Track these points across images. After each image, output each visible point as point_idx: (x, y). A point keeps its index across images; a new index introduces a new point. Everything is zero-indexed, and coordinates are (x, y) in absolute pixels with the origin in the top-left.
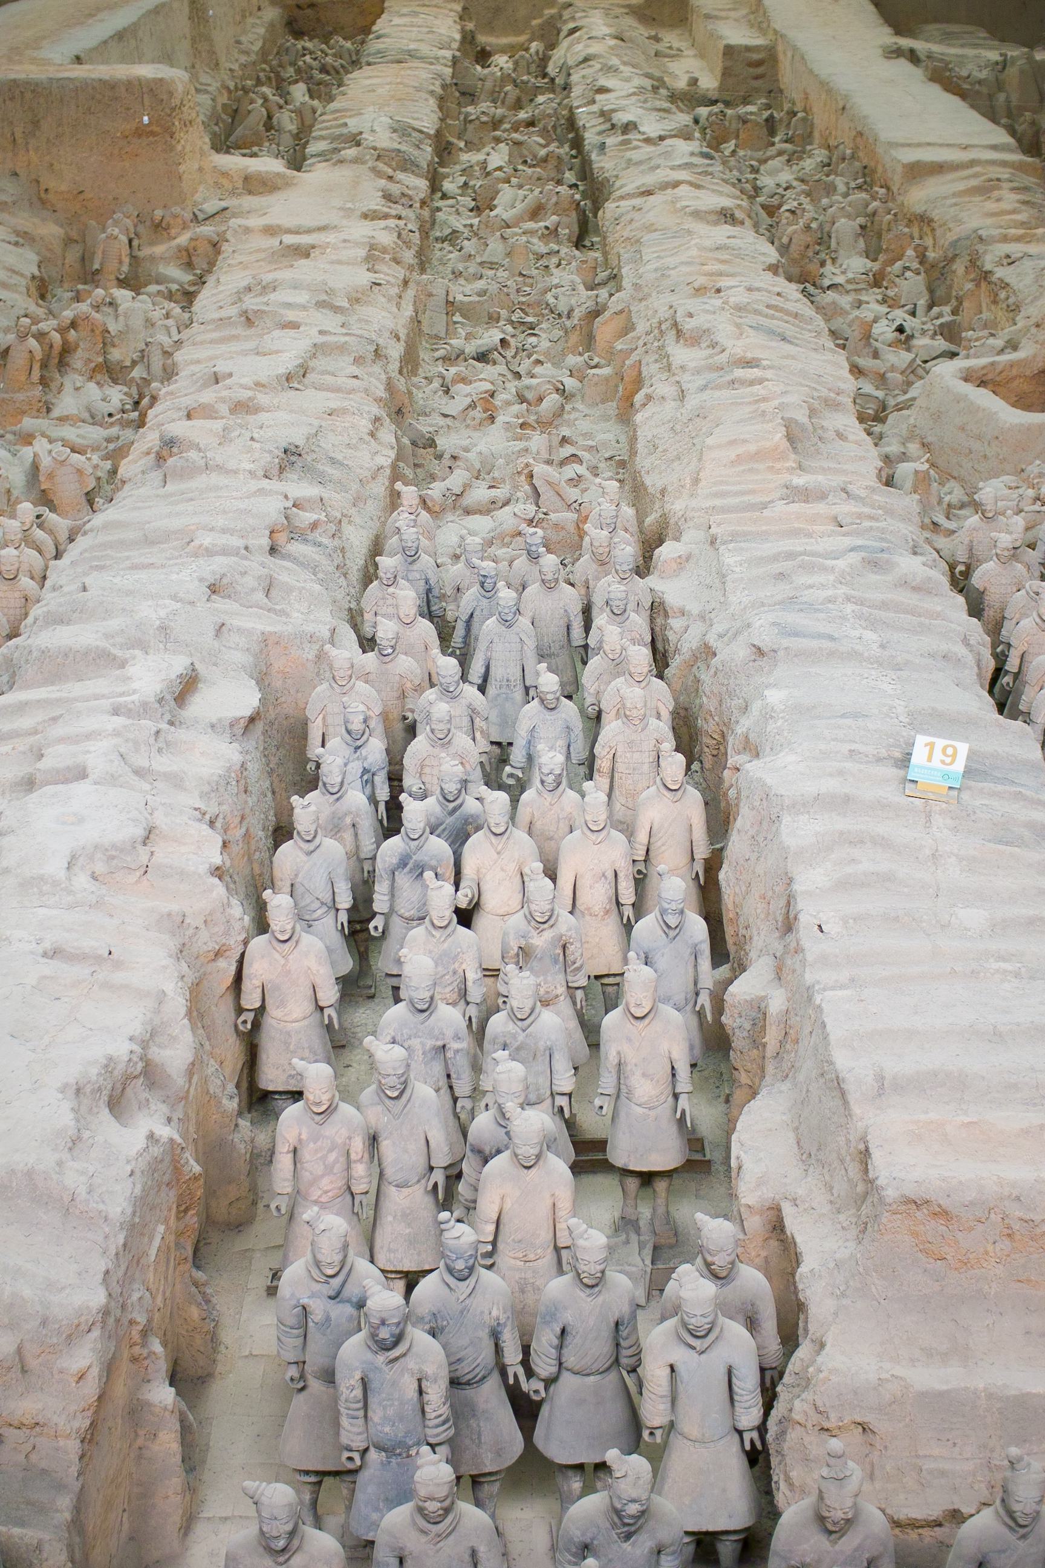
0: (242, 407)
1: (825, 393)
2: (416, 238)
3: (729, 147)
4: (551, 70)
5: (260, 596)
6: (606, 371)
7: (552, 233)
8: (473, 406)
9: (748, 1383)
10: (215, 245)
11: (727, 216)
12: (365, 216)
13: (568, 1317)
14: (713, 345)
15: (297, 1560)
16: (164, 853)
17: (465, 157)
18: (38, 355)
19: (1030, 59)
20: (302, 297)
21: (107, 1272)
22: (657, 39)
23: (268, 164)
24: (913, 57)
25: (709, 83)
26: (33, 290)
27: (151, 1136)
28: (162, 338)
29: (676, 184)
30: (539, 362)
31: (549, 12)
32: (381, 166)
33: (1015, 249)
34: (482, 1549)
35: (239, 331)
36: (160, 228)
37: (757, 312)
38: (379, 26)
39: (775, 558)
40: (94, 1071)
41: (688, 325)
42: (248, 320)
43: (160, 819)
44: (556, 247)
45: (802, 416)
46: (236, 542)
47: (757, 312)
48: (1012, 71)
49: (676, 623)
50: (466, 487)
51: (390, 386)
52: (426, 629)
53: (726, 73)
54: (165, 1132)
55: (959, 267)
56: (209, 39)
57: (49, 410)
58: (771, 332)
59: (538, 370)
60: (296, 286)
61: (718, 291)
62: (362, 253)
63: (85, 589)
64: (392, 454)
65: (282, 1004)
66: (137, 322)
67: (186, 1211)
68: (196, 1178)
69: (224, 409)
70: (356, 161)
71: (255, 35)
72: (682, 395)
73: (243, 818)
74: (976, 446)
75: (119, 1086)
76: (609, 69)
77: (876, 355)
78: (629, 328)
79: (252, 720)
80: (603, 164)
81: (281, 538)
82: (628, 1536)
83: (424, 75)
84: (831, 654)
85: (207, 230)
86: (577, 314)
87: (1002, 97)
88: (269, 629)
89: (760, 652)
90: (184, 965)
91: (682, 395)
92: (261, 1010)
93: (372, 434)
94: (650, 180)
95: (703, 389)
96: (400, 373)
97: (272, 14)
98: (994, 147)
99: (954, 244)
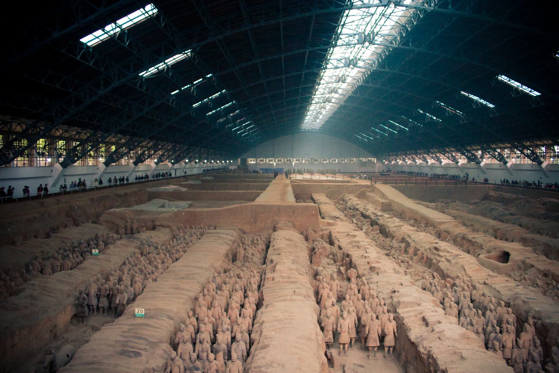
6: (416, 257)
12: (354, 230)
14: (448, 252)
20: (365, 243)
24: (420, 203)
29: (402, 225)
33: (476, 236)
35: (357, 249)
41: (442, 248)
53: (382, 207)
55: (459, 240)
60: (363, 242)
61: (437, 243)
63: (398, 292)
72: (448, 261)
78: (416, 250)
80: (381, 222)
85: (326, 232)
86: (402, 247)
91: (448, 261)
94: (397, 224)
95: (454, 259)
99: (456, 235)
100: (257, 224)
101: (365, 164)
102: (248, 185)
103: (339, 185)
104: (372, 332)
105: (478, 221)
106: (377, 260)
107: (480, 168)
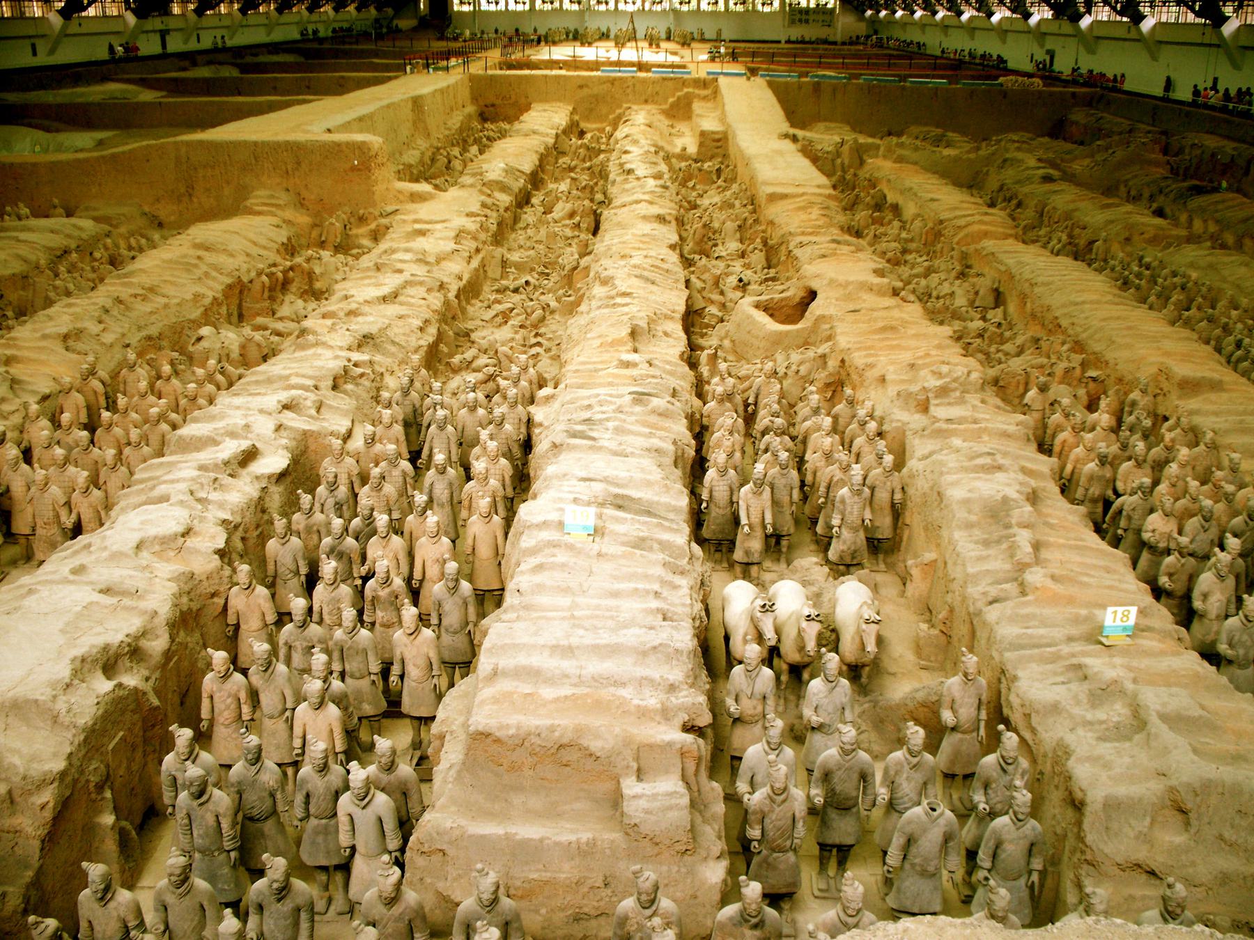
0: (352, 313)
1: (665, 311)
2: (494, 228)
3: (691, 184)
4: (612, 140)
5: (313, 412)
7: (578, 226)
8: (496, 315)
9: (390, 825)
10: (388, 228)
11: (661, 219)
12: (467, 215)
13: (309, 786)
15: (112, 905)
16: (191, 542)
17: (552, 186)
18: (267, 284)
19: (856, 140)
21: (71, 754)
22: (672, 126)
23: (424, 187)
24: (794, 139)
25: (692, 149)
26: (282, 250)
27: (120, 685)
28: (338, 277)
29: (637, 202)
30: (543, 293)
31: (618, 111)
32: (485, 189)
33: (805, 239)
34: (205, 904)
36: (362, 220)
37: (644, 269)
38: (525, 117)
39: (589, 397)
40: (95, 651)
42: (378, 268)
43: (197, 525)
44: (576, 233)
45: (643, 324)
46: (310, 383)
47: (644, 269)
48: (846, 148)
49: (537, 431)
50: (475, 358)
51: (447, 303)
52: (398, 429)
53: (701, 145)
54: (131, 680)
55: (783, 248)
56: (424, 122)
57: (274, 314)
58: (647, 280)
59: (542, 298)
60: (407, 250)
62: (453, 234)
64: (431, 340)
65: (246, 623)
66: (332, 268)
67: (153, 726)
68: (157, 708)
69: (342, 314)
70: (472, 186)
71: (456, 120)
73: (258, 526)
74: (756, 343)
75: (112, 661)
76: (635, 142)
77: (722, 293)
79: (282, 476)
80: (613, 190)
81: (341, 381)
82: (279, 900)
83: (536, 142)
84: (591, 448)
85: (384, 221)
87: (839, 161)
88: (307, 427)
89: (555, 446)
90: (185, 600)
92: (237, 627)
93: (421, 329)
95: (599, 307)
96: (457, 297)
97: (471, 109)
98: (819, 187)
100: (195, 200)
101: (804, 17)
102: (343, 77)
103: (615, 79)
104: (40, 523)
105: (916, 195)
106: (354, 306)
107: (1078, 34)
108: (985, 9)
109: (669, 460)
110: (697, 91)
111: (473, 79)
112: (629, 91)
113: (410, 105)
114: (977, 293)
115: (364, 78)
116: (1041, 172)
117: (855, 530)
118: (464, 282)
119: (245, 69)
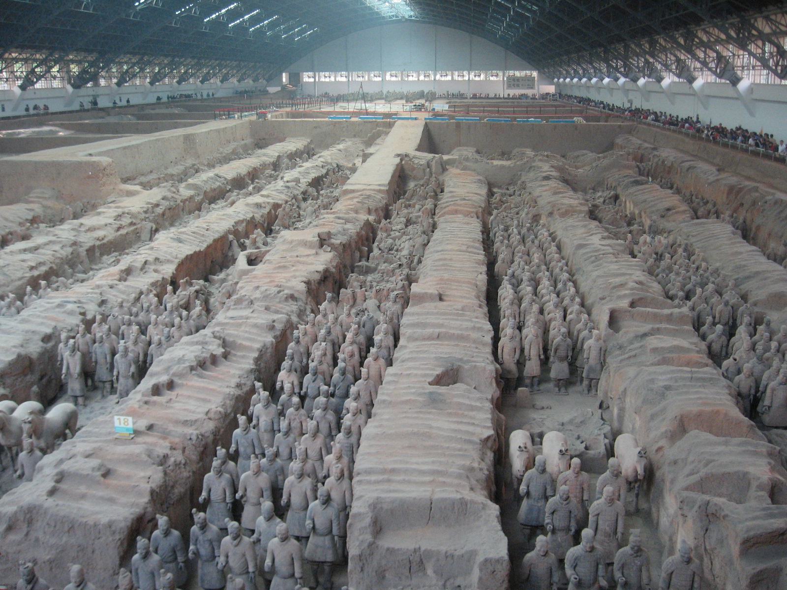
1: (169, 257)
19: (441, 158)
37: (186, 234)
48: (434, 161)
71: (228, 149)
97: (249, 141)
98: (379, 185)
101: (516, 83)
103: (336, 123)
108: (654, 75)
109: (38, 338)
110: (384, 130)
111: (251, 122)
112: (344, 129)
113: (182, 139)
114: (414, 246)
115: (189, 123)
116: (544, 174)
117: (126, 377)
118: (105, 241)
119: (139, 117)
